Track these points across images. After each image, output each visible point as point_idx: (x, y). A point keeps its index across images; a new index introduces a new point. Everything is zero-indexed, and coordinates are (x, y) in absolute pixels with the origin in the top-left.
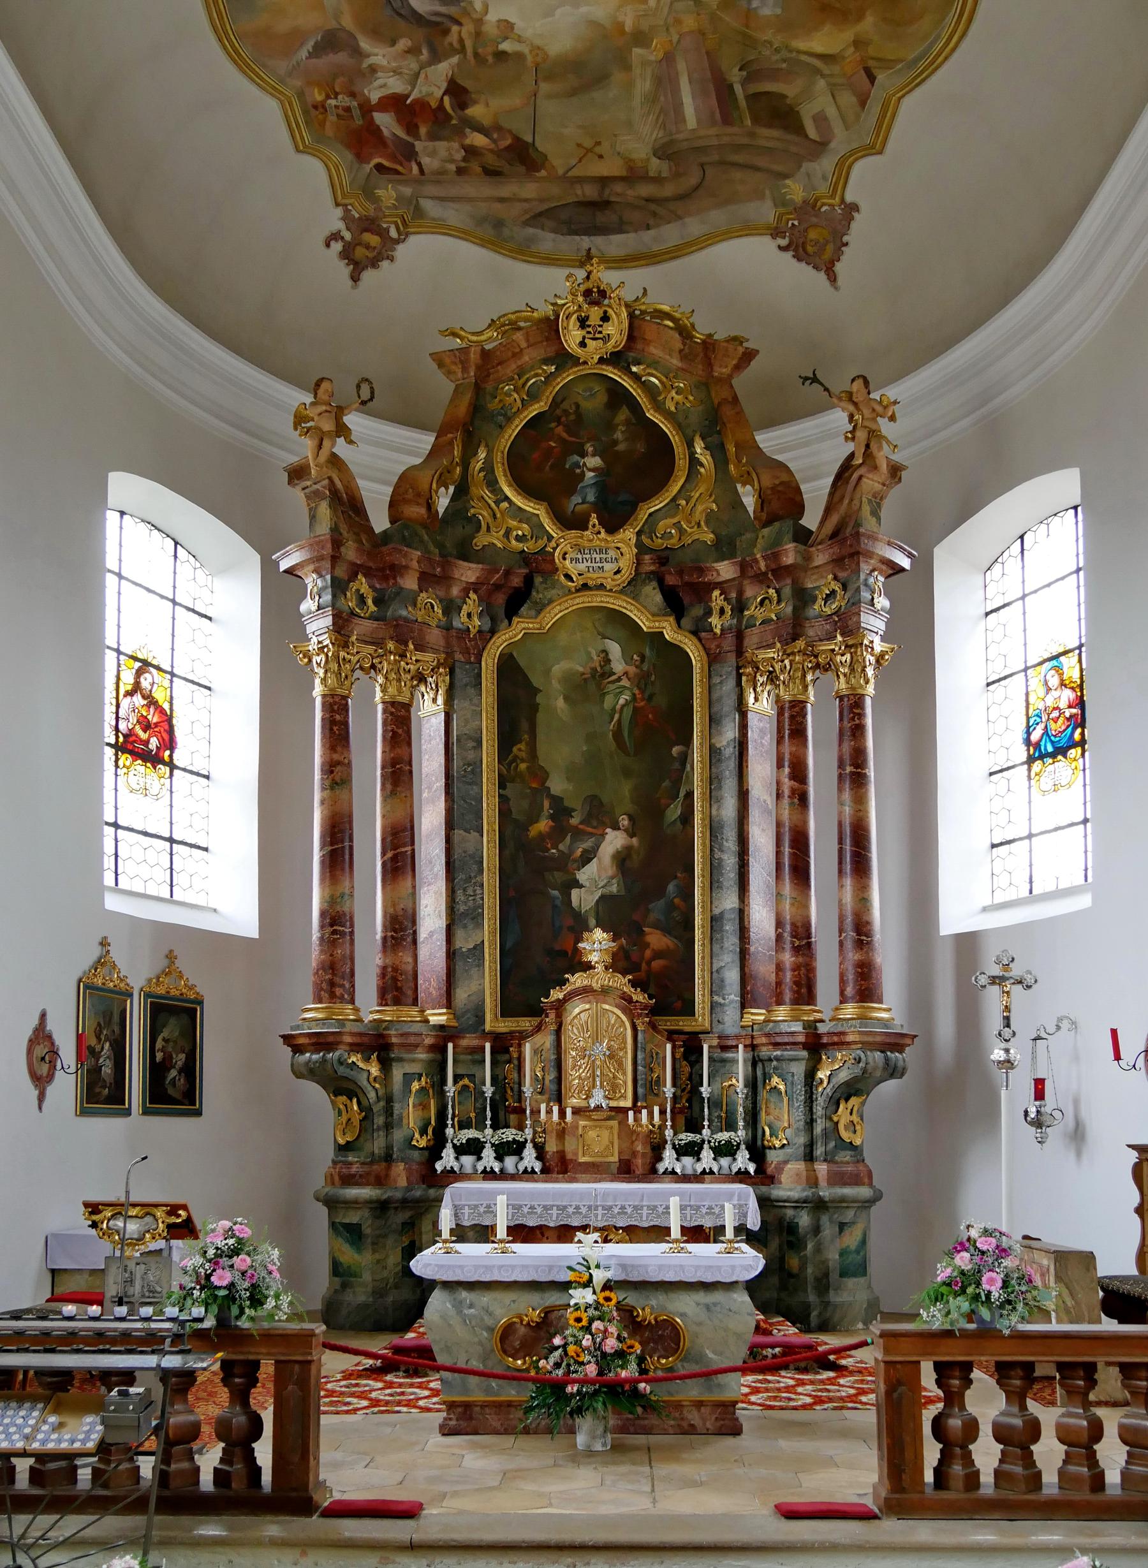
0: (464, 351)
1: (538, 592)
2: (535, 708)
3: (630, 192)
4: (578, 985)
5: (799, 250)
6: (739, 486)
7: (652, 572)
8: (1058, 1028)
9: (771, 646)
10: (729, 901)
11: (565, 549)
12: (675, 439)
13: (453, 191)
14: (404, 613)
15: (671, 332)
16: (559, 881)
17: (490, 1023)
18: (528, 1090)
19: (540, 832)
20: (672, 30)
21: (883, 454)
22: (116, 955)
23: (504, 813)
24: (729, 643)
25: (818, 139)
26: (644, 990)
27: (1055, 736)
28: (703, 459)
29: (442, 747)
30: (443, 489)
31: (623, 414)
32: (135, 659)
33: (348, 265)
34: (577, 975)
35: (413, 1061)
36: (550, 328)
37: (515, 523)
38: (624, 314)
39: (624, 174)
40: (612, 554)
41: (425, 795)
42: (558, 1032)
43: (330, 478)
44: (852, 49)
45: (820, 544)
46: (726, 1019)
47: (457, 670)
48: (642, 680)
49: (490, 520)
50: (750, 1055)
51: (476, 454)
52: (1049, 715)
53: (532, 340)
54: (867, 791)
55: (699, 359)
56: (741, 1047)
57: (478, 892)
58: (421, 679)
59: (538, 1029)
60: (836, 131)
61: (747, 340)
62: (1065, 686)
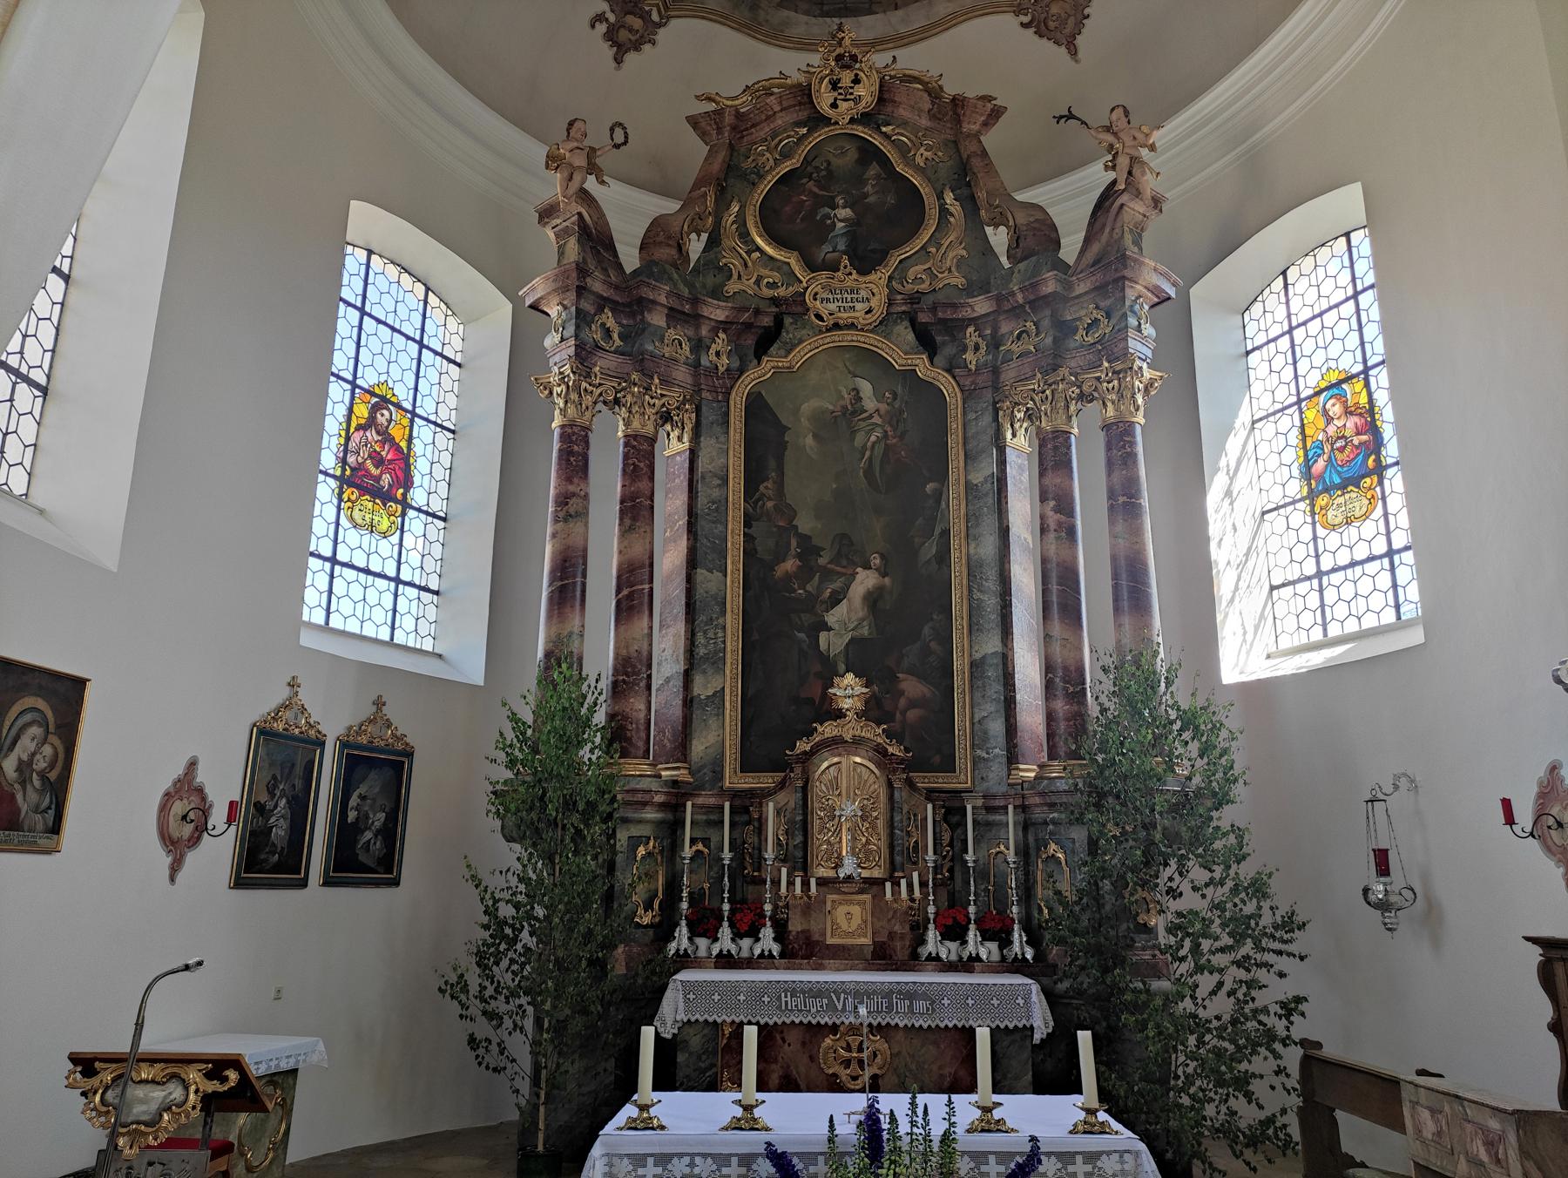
0: (719, 113)
1: (788, 332)
2: (783, 446)
4: (826, 736)
5: (1041, 27)
6: (989, 230)
7: (904, 312)
8: (1396, 787)
10: (990, 645)
11: (816, 290)
12: (925, 190)
14: (650, 347)
15: (921, 93)
16: (806, 624)
17: (733, 779)
18: (769, 854)
19: (787, 572)
21: (1149, 183)
22: (304, 696)
23: (749, 554)
24: (984, 379)
26: (900, 742)
27: (1342, 466)
28: (952, 209)
29: (686, 484)
30: (693, 236)
31: (874, 170)
32: (373, 394)
34: (826, 724)
35: (640, 821)
36: (804, 94)
37: (767, 272)
38: (875, 77)
40: (863, 293)
42: (805, 789)
43: (580, 214)
45: (1081, 272)
46: (991, 775)
47: (704, 409)
48: (894, 418)
49: (741, 269)
50: (1021, 818)
52: (1332, 444)
53: (785, 104)
54: (1142, 524)
55: (948, 117)
56: (1011, 808)
57: (720, 635)
58: (666, 417)
59: (782, 785)
61: (995, 99)
62: (1351, 413)
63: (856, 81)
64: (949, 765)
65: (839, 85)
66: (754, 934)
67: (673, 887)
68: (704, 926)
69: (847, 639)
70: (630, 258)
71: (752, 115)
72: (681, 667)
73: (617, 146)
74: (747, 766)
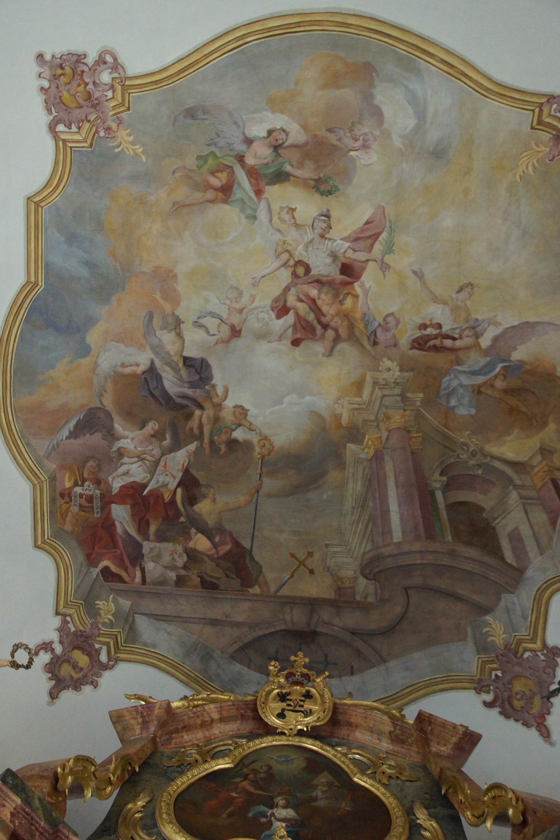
3: (336, 621)
12: (389, 800)
13: (170, 608)
20: (382, 425)
25: (515, 564)
31: (324, 778)
33: (50, 679)
39: (332, 596)
44: (539, 458)
53: (225, 714)
60: (531, 555)
65: (289, 697)
71: (186, 718)
73: (15, 665)
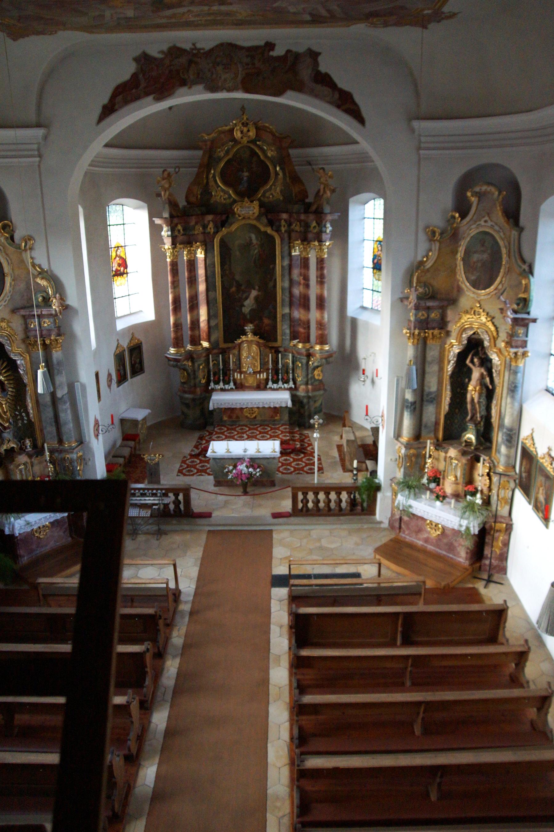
0: (205, 141)
9: (297, 240)
17: (222, 345)
29: (204, 267)
31: (255, 159)
36: (231, 131)
40: (252, 208)
41: (200, 280)
51: (210, 171)
59: (234, 348)
63: (248, 131)
64: (276, 340)
66: (228, 383)
67: (209, 372)
68: (217, 382)
69: (250, 309)
70: (182, 203)
72: (207, 319)
74: (225, 341)
